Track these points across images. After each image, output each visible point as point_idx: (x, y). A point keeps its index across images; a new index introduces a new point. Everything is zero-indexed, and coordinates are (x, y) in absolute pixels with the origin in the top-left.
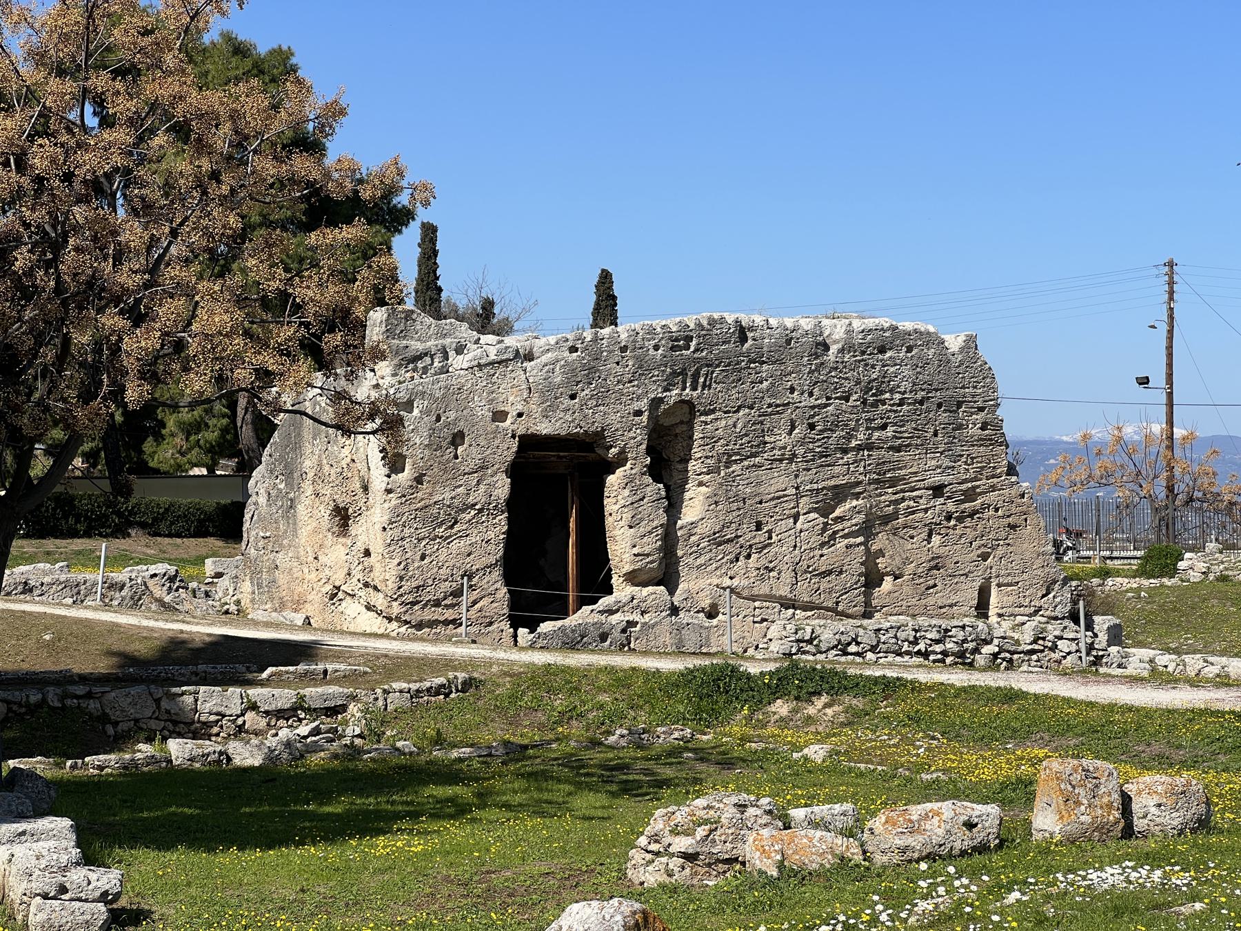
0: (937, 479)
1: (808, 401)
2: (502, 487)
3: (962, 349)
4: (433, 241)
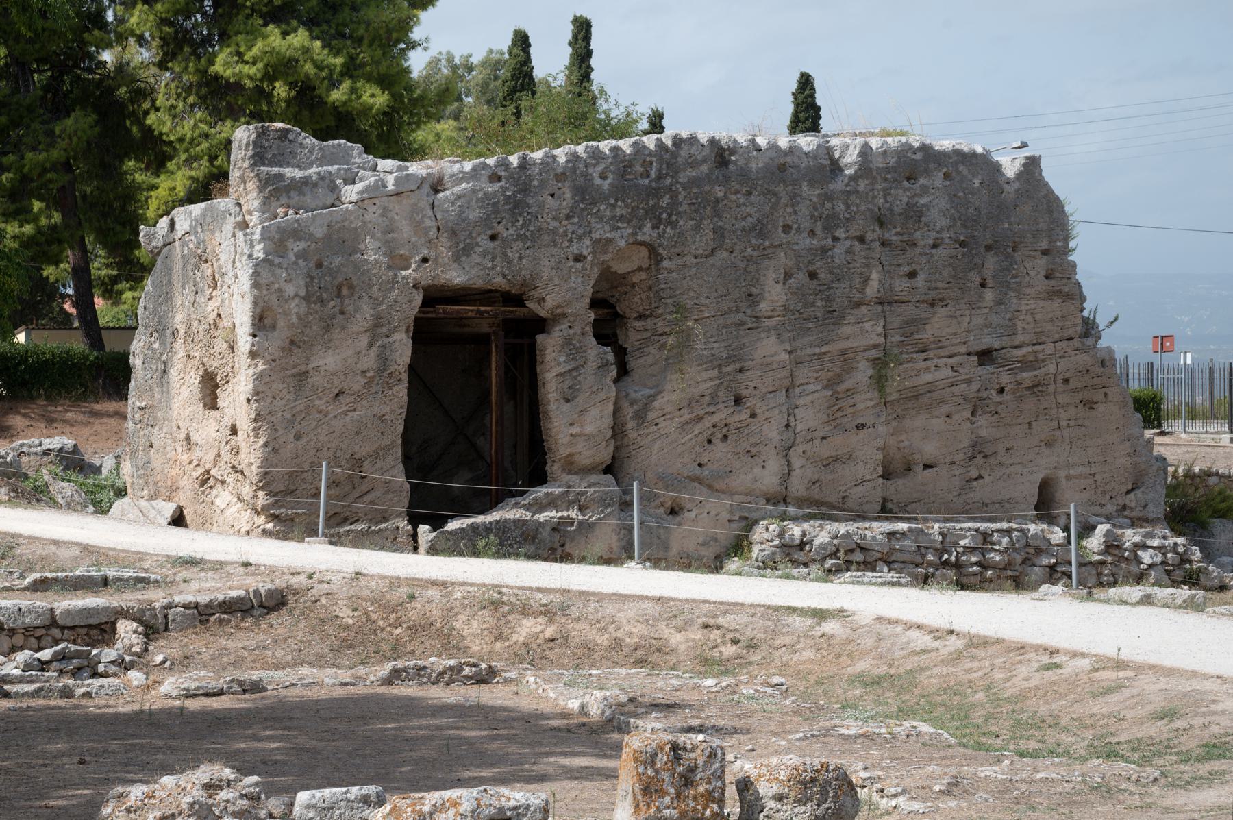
1: (806, 242)
3: (1019, 176)
4: (587, 38)
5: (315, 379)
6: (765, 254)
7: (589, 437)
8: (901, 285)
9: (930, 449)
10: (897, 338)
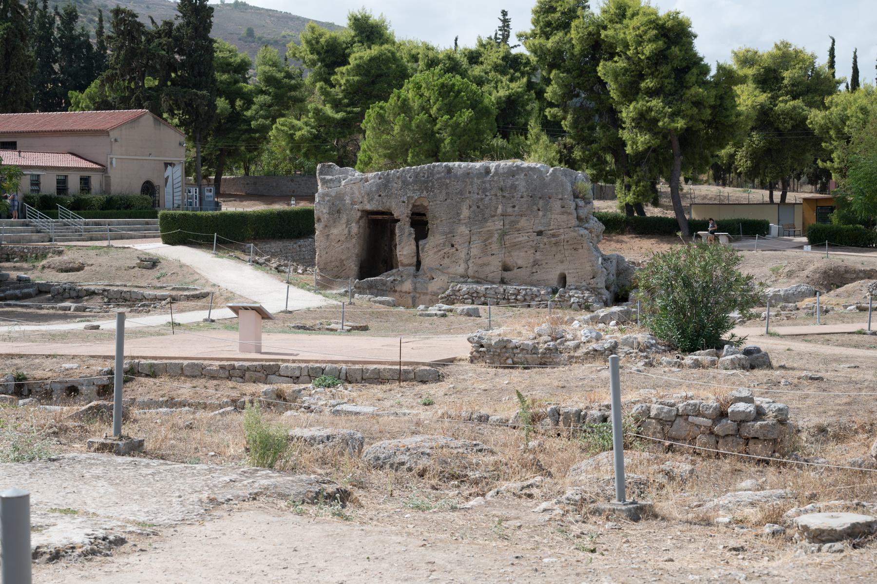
0: (540, 228)
1: (476, 196)
2: (355, 228)
5: (332, 237)
6: (463, 200)
7: (405, 255)
8: (510, 210)
9: (520, 262)
10: (508, 227)
